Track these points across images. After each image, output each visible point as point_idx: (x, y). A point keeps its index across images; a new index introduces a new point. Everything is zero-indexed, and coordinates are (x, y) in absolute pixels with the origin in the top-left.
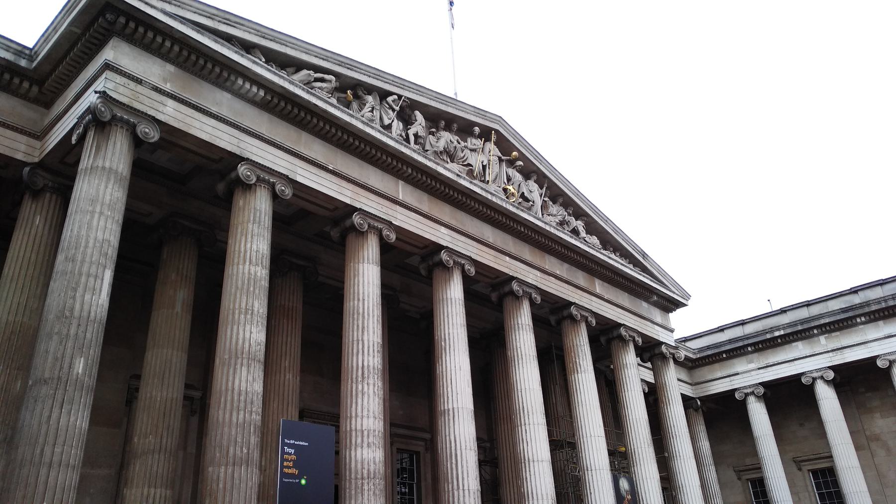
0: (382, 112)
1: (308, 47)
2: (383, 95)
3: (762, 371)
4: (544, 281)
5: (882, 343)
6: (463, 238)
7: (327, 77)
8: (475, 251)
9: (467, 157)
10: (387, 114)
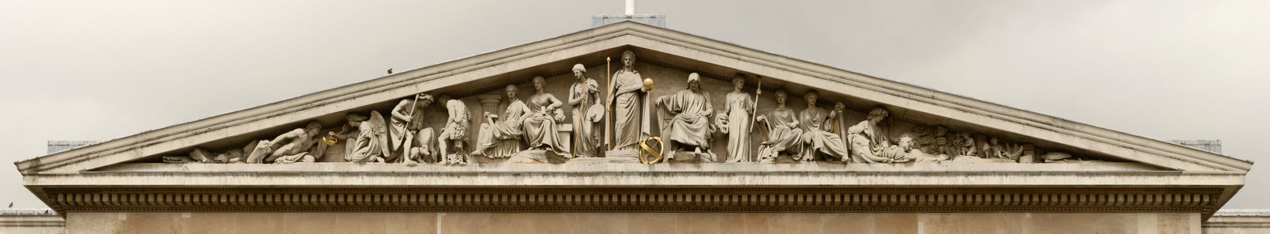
1: (254, 113)
2: (385, 110)
7: (290, 134)
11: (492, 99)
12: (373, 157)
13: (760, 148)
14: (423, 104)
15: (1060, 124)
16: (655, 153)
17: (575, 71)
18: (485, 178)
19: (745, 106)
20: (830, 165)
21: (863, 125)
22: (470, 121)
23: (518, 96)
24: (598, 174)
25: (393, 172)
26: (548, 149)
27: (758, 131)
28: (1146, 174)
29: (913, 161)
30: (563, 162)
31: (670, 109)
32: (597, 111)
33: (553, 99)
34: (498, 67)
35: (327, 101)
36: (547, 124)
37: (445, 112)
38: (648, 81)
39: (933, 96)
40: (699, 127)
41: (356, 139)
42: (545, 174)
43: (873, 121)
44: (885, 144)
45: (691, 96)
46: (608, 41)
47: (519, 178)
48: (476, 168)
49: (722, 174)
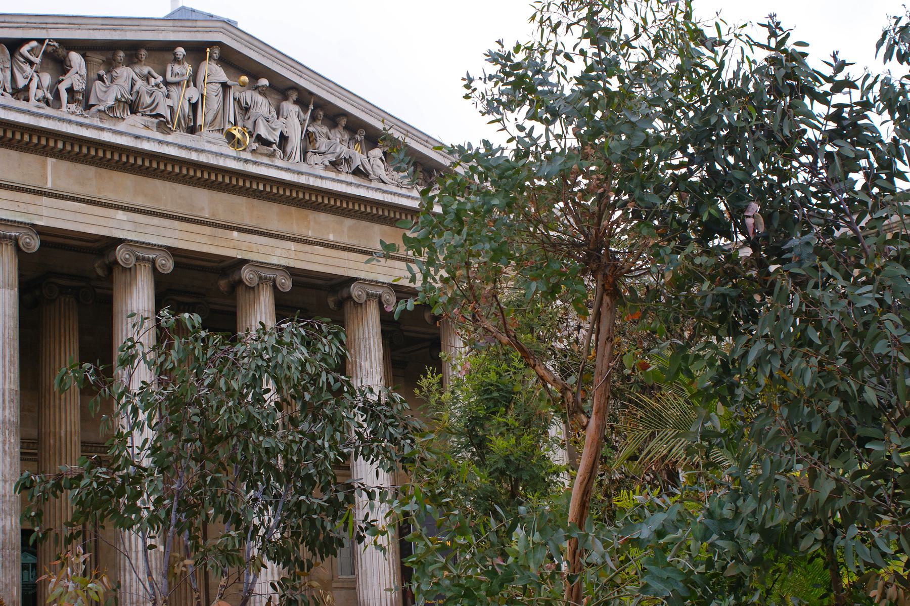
0: (15, 70)
4: (302, 256)
6: (156, 221)
8: (177, 234)
9: (158, 104)
10: (22, 71)
13: (309, 154)
17: (179, 53)
18: (110, 134)
20: (361, 180)
24: (203, 151)
25: (29, 111)
30: (169, 134)
32: (193, 93)
34: (119, 32)
40: (277, 127)
45: (260, 98)
46: (206, 34)
47: (139, 141)
48: (96, 122)
49: (293, 172)
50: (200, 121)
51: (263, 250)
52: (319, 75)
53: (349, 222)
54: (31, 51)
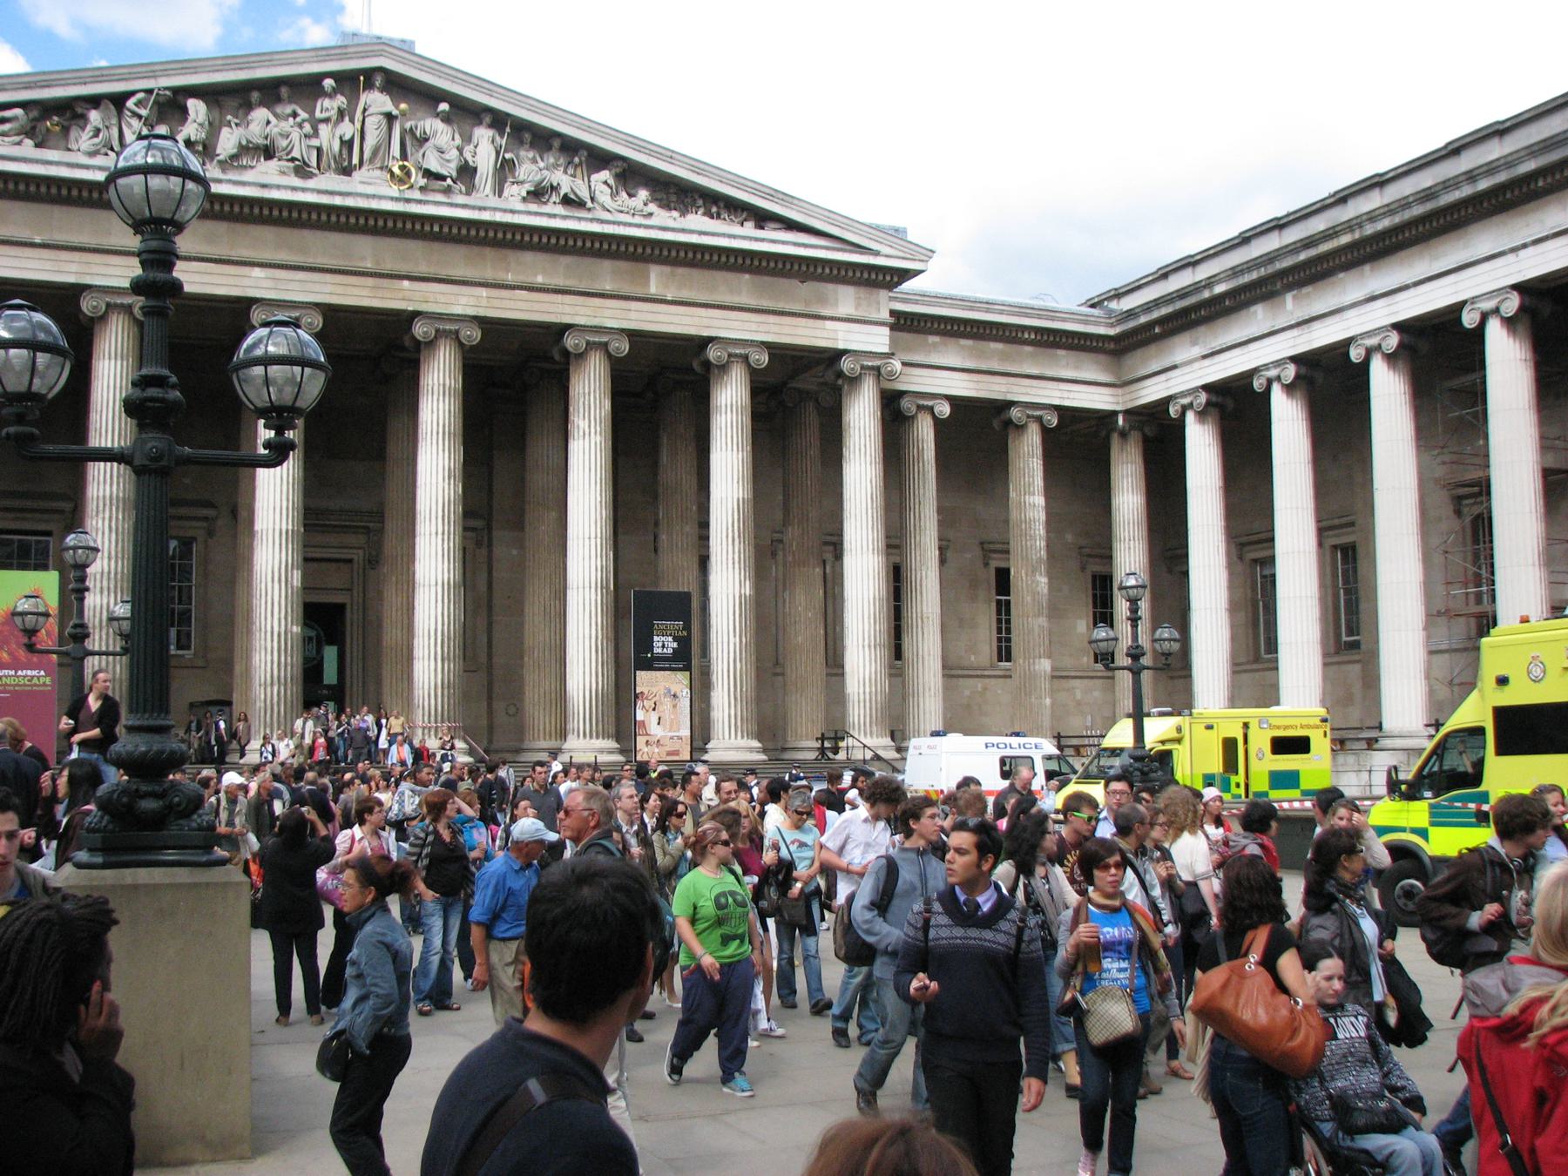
2: (118, 101)
3: (1207, 362)
4: (496, 303)
5: (1362, 311)
8: (329, 289)
10: (130, 126)
11: (232, 103)
12: (104, 150)
13: (506, 185)
14: (161, 99)
15: (781, 196)
16: (406, 178)
17: (326, 86)
19: (493, 142)
21: (605, 175)
22: (210, 124)
23: (262, 104)
26: (297, 163)
27: (505, 169)
28: (851, 252)
29: (651, 214)
30: (311, 178)
31: (418, 135)
32: (347, 129)
33: (299, 111)
35: (54, 83)
36: (296, 135)
37: (184, 112)
38: (403, 106)
39: (671, 156)
41: (83, 129)
42: (294, 189)
43: (613, 171)
44: (624, 195)
45: (438, 125)
49: (473, 208)
50: (355, 160)
51: (442, 299)
52: (515, 92)
53: (566, 260)
54: (139, 104)
